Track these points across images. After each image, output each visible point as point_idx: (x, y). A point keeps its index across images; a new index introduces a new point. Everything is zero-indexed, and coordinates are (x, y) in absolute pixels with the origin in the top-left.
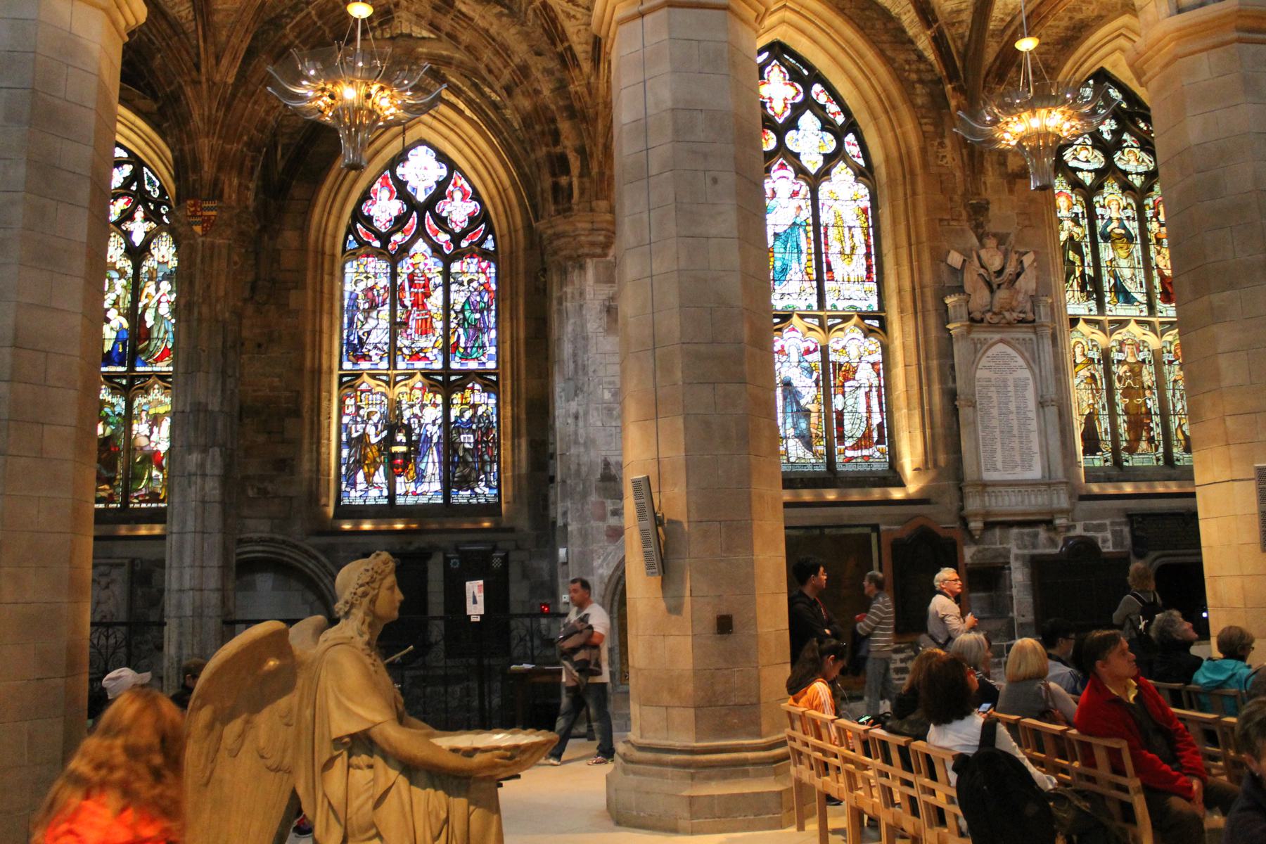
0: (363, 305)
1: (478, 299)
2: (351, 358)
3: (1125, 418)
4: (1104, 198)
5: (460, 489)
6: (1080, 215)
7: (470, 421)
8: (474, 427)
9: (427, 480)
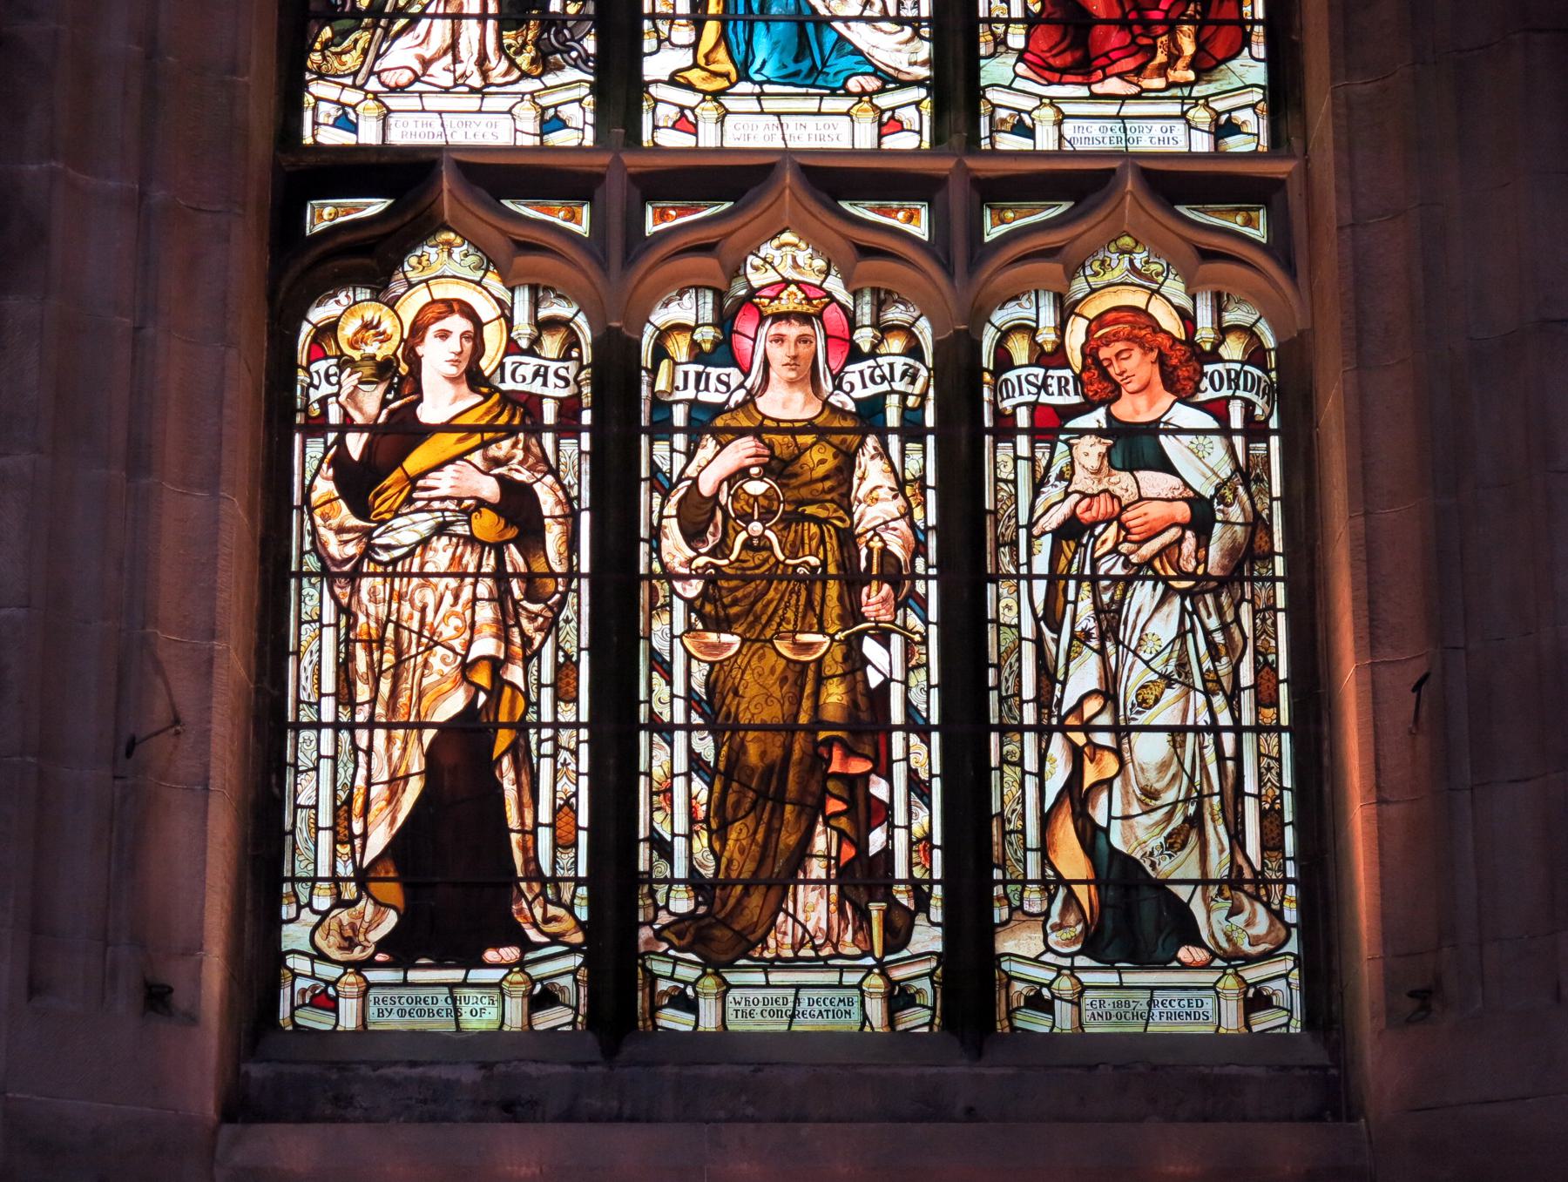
3: (705, 746)
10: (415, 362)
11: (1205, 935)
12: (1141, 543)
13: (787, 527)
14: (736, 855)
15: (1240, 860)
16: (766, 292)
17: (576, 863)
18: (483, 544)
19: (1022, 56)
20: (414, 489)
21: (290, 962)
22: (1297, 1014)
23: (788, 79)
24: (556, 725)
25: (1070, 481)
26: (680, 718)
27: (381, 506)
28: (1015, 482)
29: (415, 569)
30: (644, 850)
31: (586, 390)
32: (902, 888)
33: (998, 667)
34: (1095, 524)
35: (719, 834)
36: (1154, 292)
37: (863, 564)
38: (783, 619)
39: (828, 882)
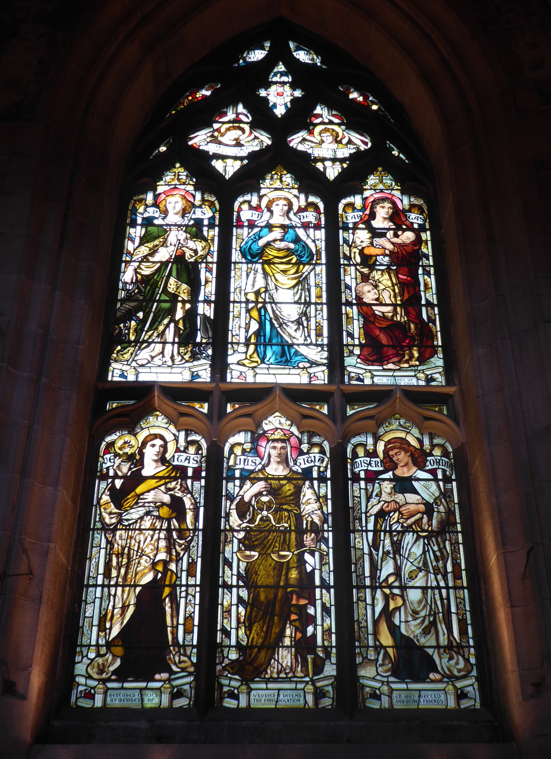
3: (244, 593)
4: (261, 198)
6: (206, 222)
10: (142, 455)
11: (439, 669)
12: (407, 519)
13: (276, 513)
14: (255, 636)
15: (452, 638)
16: (270, 432)
17: (192, 639)
18: (163, 519)
19: (359, 356)
20: (139, 499)
21: (77, 679)
22: (478, 700)
23: (278, 363)
24: (187, 586)
25: (380, 497)
26: (235, 583)
27: (126, 505)
28: (360, 497)
29: (137, 527)
30: (219, 634)
31: (204, 465)
32: (320, 649)
33: (356, 564)
34: (390, 512)
35: (249, 628)
36: (408, 433)
37: (305, 526)
38: (275, 546)
39: (291, 647)
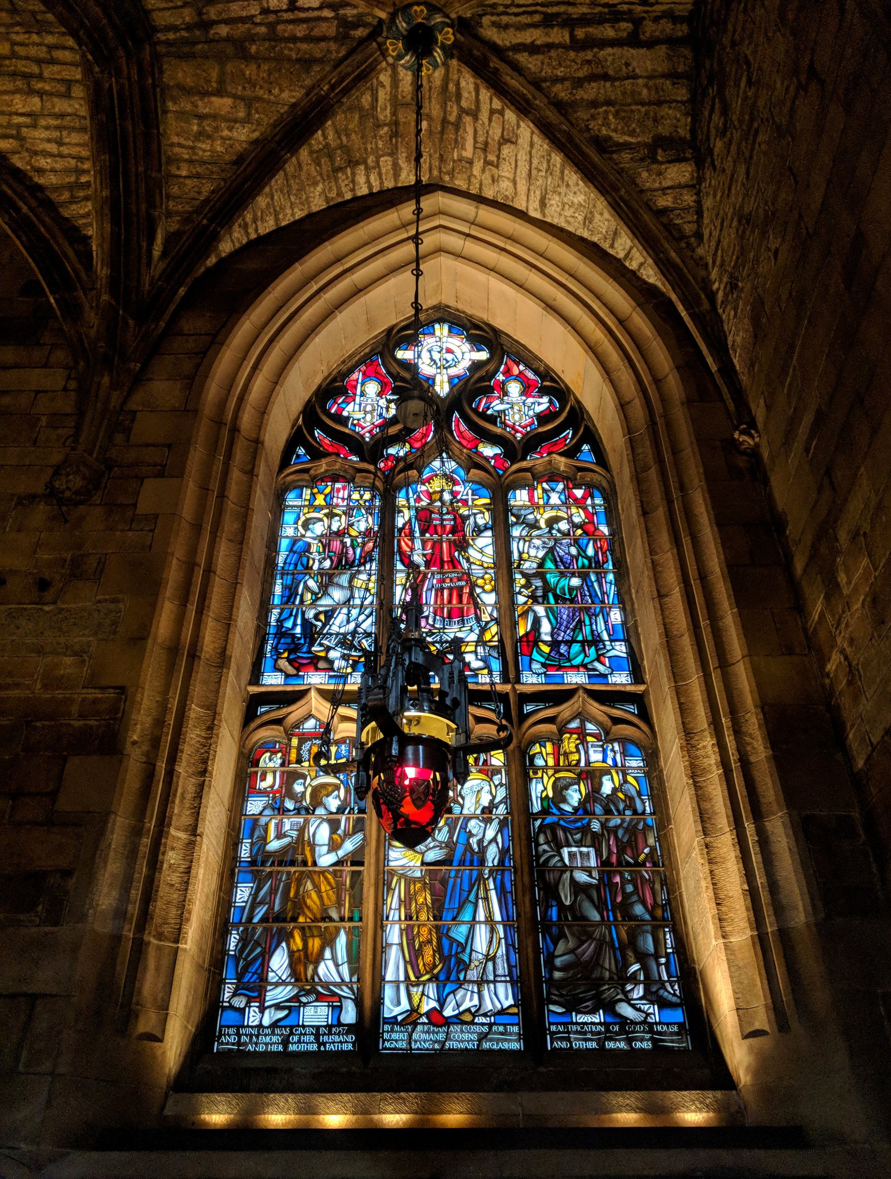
0: (319, 562)
1: (574, 551)
2: (283, 663)
5: (573, 1006)
7: (584, 807)
8: (596, 826)
9: (473, 975)
